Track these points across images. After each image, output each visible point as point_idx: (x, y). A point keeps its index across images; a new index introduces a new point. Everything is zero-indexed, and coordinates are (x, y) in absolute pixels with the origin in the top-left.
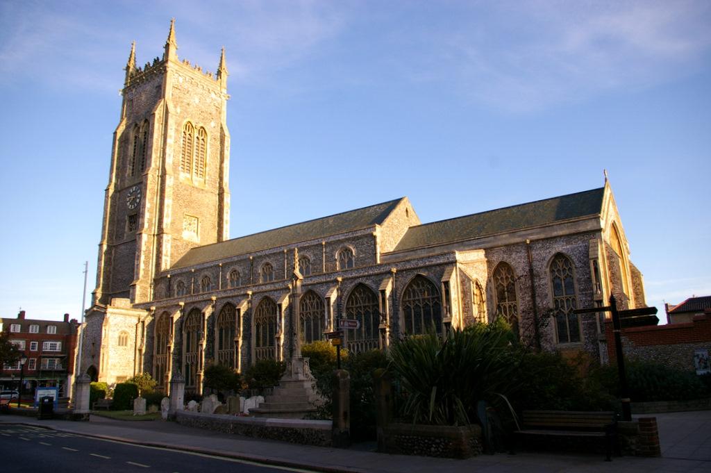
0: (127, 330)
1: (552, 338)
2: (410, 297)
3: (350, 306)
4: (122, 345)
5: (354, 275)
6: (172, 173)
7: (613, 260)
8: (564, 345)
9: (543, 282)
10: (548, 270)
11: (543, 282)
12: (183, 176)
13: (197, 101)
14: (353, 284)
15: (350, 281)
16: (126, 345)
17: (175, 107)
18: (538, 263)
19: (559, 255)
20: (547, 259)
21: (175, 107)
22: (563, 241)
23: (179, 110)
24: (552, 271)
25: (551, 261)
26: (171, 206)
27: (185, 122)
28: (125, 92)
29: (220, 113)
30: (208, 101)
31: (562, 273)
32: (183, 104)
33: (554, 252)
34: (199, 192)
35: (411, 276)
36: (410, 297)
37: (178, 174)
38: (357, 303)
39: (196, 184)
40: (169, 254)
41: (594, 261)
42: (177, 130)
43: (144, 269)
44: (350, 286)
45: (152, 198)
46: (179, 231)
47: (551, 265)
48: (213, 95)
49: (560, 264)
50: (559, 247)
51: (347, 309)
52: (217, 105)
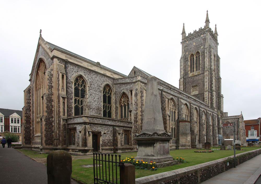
27: (190, 56)
34: (197, 76)
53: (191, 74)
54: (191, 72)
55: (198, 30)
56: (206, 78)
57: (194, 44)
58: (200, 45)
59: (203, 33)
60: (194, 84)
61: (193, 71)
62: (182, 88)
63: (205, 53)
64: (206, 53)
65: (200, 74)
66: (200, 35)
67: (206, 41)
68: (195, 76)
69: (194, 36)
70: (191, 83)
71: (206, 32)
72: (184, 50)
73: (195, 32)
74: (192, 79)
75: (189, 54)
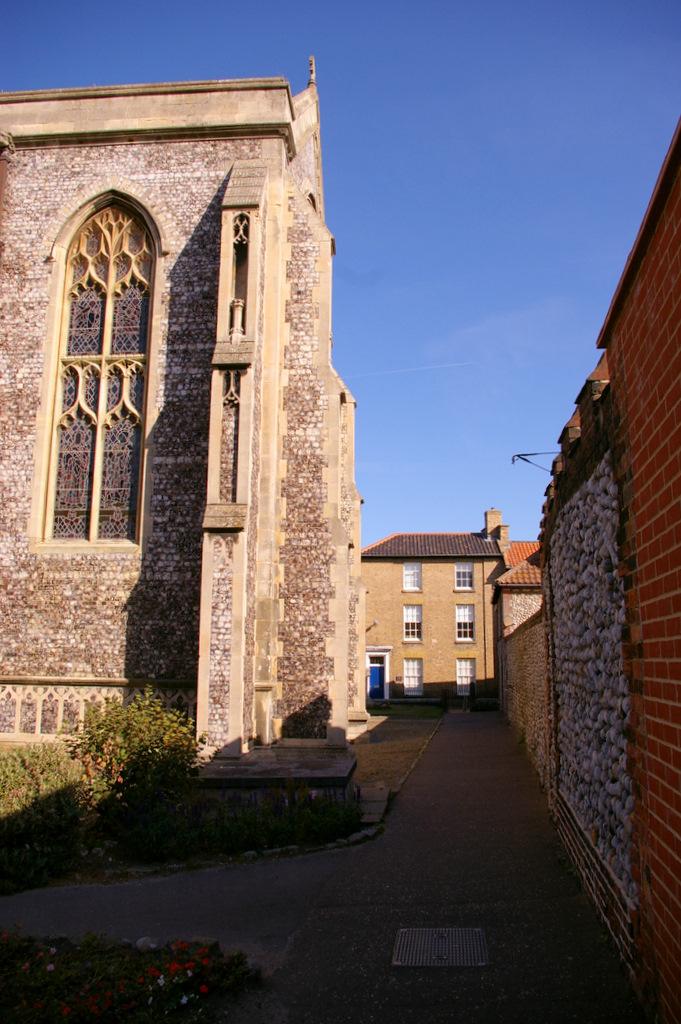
1: (24, 517)
7: (307, 245)
8: (73, 548)
9: (31, 295)
10: (60, 253)
11: (31, 295)
18: (29, 224)
19: (118, 203)
20: (65, 213)
22: (135, 155)
24: (82, 262)
25: (79, 221)
31: (113, 271)
33: (95, 190)
41: (242, 218)
47: (77, 238)
49: (118, 237)
50: (124, 171)
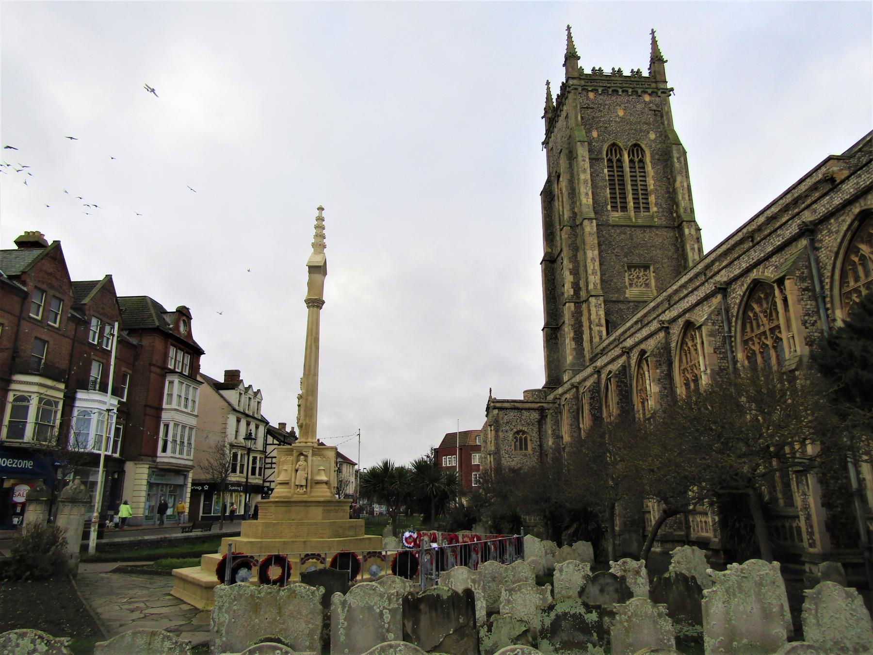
0: (525, 429)
2: (857, 279)
3: (749, 335)
4: (521, 449)
5: (744, 266)
6: (592, 215)
12: (615, 216)
13: (621, 113)
14: (746, 286)
15: (739, 283)
16: (526, 449)
17: (588, 131)
21: (588, 131)
23: (595, 134)
26: (597, 260)
27: (605, 147)
28: (545, 143)
29: (662, 117)
30: (639, 107)
32: (601, 124)
34: (645, 231)
35: (846, 220)
36: (857, 279)
37: (608, 216)
38: (758, 326)
39: (640, 222)
40: (603, 322)
42: (594, 160)
43: (575, 349)
44: (739, 291)
45: (575, 256)
46: (621, 290)
48: (647, 98)
51: (745, 342)
52: (654, 108)
53: (616, 214)
54: (614, 208)
55: (627, 73)
56: (693, 249)
57: (621, 113)
58: (645, 127)
59: (649, 91)
60: (636, 260)
61: (624, 208)
62: (593, 259)
63: (676, 160)
64: (678, 159)
65: (657, 227)
66: (639, 91)
67: (666, 123)
68: (638, 230)
69: (621, 88)
70: (622, 248)
71: (662, 93)
72: (582, 118)
73: (617, 73)
74: (625, 234)
75: (603, 141)
